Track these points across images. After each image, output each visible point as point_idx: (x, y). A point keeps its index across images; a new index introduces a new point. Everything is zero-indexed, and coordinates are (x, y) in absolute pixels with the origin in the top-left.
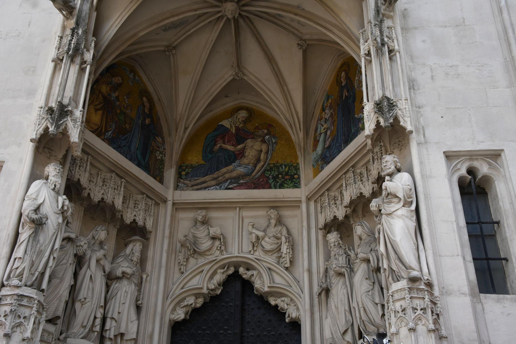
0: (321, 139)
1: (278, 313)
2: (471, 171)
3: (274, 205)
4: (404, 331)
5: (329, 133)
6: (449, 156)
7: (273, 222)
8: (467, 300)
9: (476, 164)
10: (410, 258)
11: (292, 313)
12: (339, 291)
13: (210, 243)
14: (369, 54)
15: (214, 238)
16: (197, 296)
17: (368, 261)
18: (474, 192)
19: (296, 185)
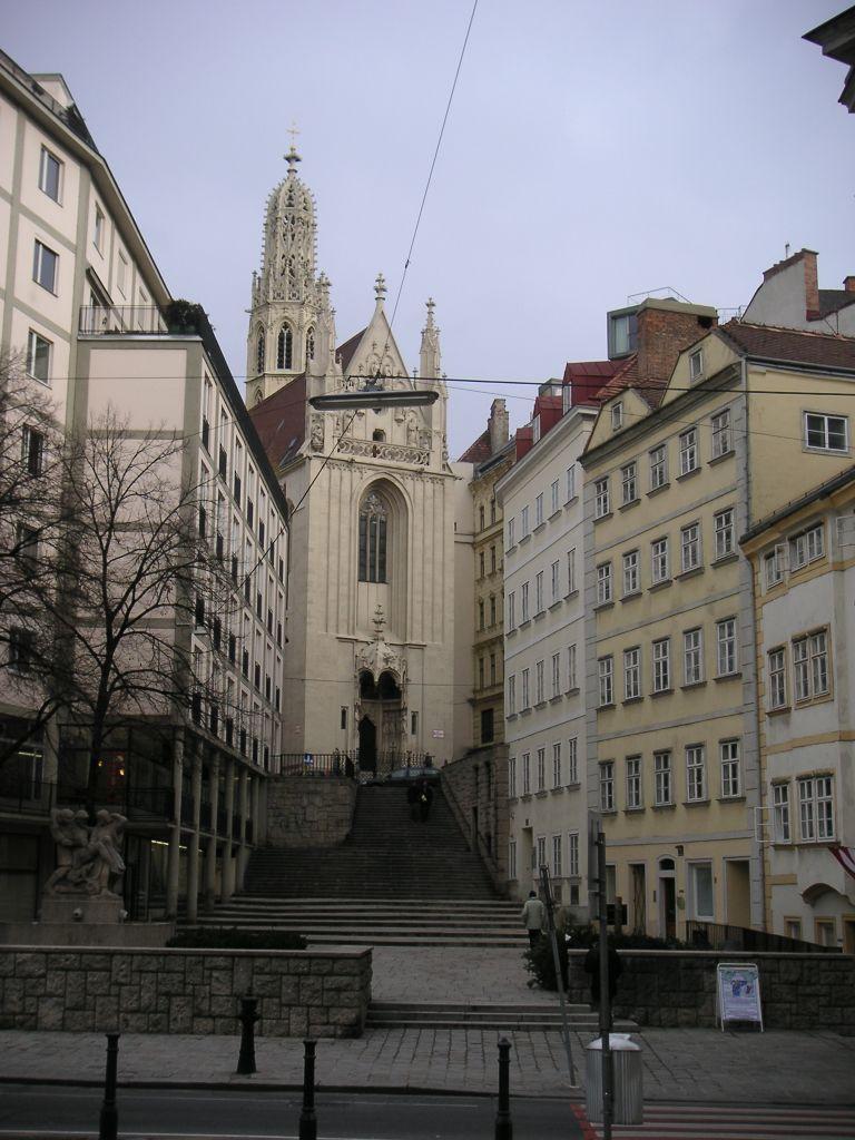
18: (414, 717)
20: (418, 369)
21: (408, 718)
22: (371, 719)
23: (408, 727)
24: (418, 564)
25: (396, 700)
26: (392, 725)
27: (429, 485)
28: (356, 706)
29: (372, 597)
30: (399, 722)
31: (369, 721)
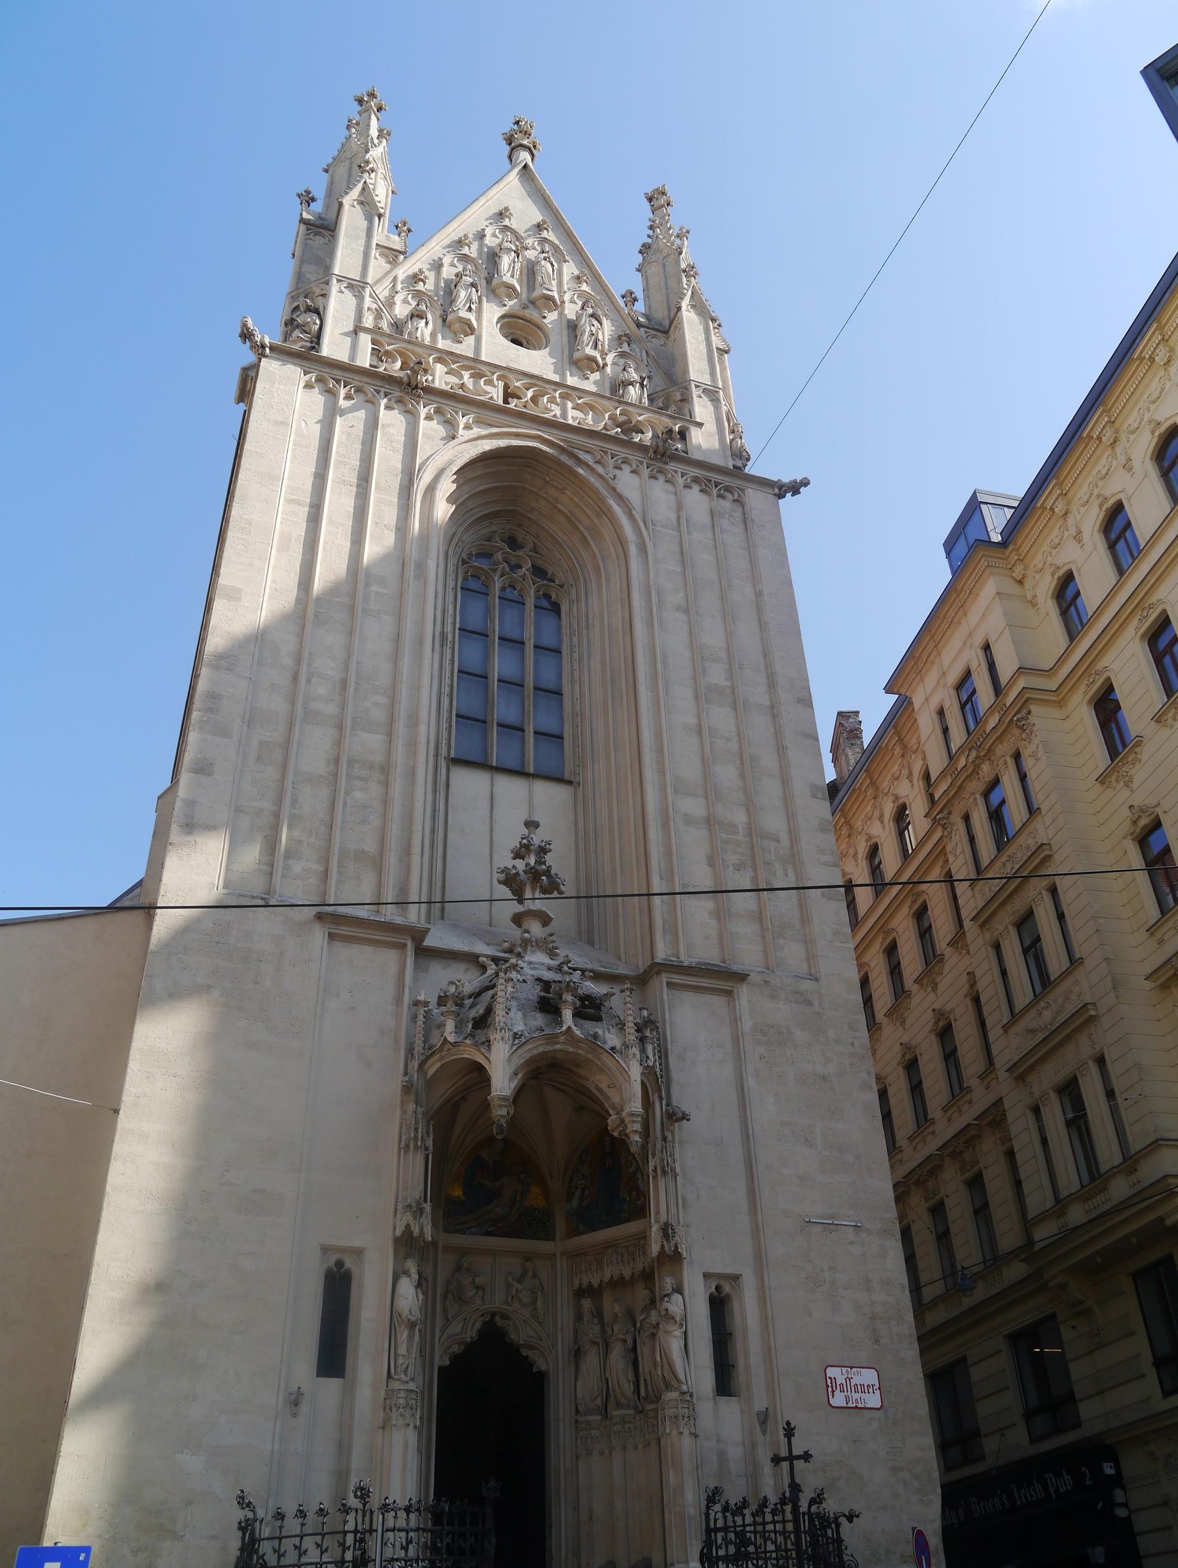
0: (578, 1194)
1: (528, 1364)
2: (718, 1288)
3: (528, 1258)
4: (675, 1432)
5: (587, 1192)
6: (706, 1276)
7: (530, 1274)
8: (711, 1404)
9: (722, 1283)
10: (682, 1376)
11: (541, 1365)
12: (591, 1359)
13: (474, 1291)
14: (655, 1171)
15: (478, 1288)
16: (460, 1344)
17: (625, 1341)
18: (719, 1305)
19: (550, 1237)
20: (639, 294)
21: (691, 1304)
22: (521, 1333)
23: (688, 1353)
24: (682, 697)
25: (632, 1227)
26: (617, 1360)
27: (695, 499)
28: (406, 1244)
29: (498, 813)
30: (641, 1333)
31: (513, 1351)
